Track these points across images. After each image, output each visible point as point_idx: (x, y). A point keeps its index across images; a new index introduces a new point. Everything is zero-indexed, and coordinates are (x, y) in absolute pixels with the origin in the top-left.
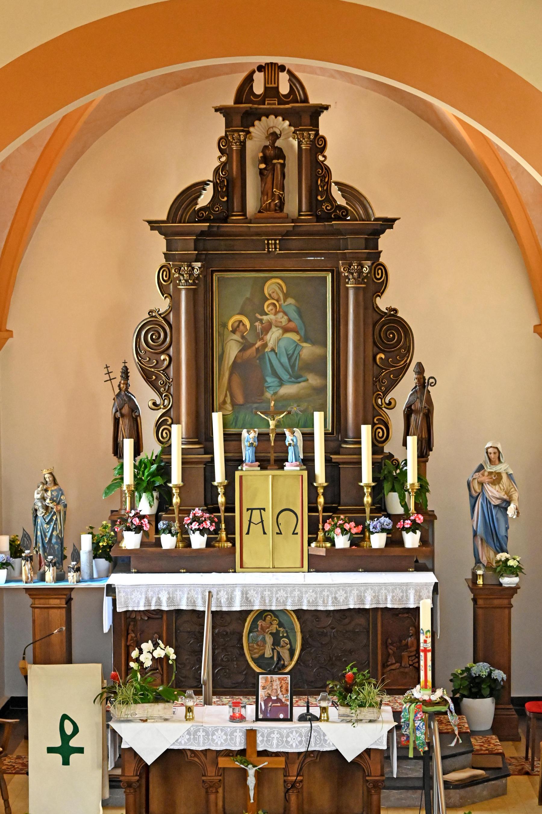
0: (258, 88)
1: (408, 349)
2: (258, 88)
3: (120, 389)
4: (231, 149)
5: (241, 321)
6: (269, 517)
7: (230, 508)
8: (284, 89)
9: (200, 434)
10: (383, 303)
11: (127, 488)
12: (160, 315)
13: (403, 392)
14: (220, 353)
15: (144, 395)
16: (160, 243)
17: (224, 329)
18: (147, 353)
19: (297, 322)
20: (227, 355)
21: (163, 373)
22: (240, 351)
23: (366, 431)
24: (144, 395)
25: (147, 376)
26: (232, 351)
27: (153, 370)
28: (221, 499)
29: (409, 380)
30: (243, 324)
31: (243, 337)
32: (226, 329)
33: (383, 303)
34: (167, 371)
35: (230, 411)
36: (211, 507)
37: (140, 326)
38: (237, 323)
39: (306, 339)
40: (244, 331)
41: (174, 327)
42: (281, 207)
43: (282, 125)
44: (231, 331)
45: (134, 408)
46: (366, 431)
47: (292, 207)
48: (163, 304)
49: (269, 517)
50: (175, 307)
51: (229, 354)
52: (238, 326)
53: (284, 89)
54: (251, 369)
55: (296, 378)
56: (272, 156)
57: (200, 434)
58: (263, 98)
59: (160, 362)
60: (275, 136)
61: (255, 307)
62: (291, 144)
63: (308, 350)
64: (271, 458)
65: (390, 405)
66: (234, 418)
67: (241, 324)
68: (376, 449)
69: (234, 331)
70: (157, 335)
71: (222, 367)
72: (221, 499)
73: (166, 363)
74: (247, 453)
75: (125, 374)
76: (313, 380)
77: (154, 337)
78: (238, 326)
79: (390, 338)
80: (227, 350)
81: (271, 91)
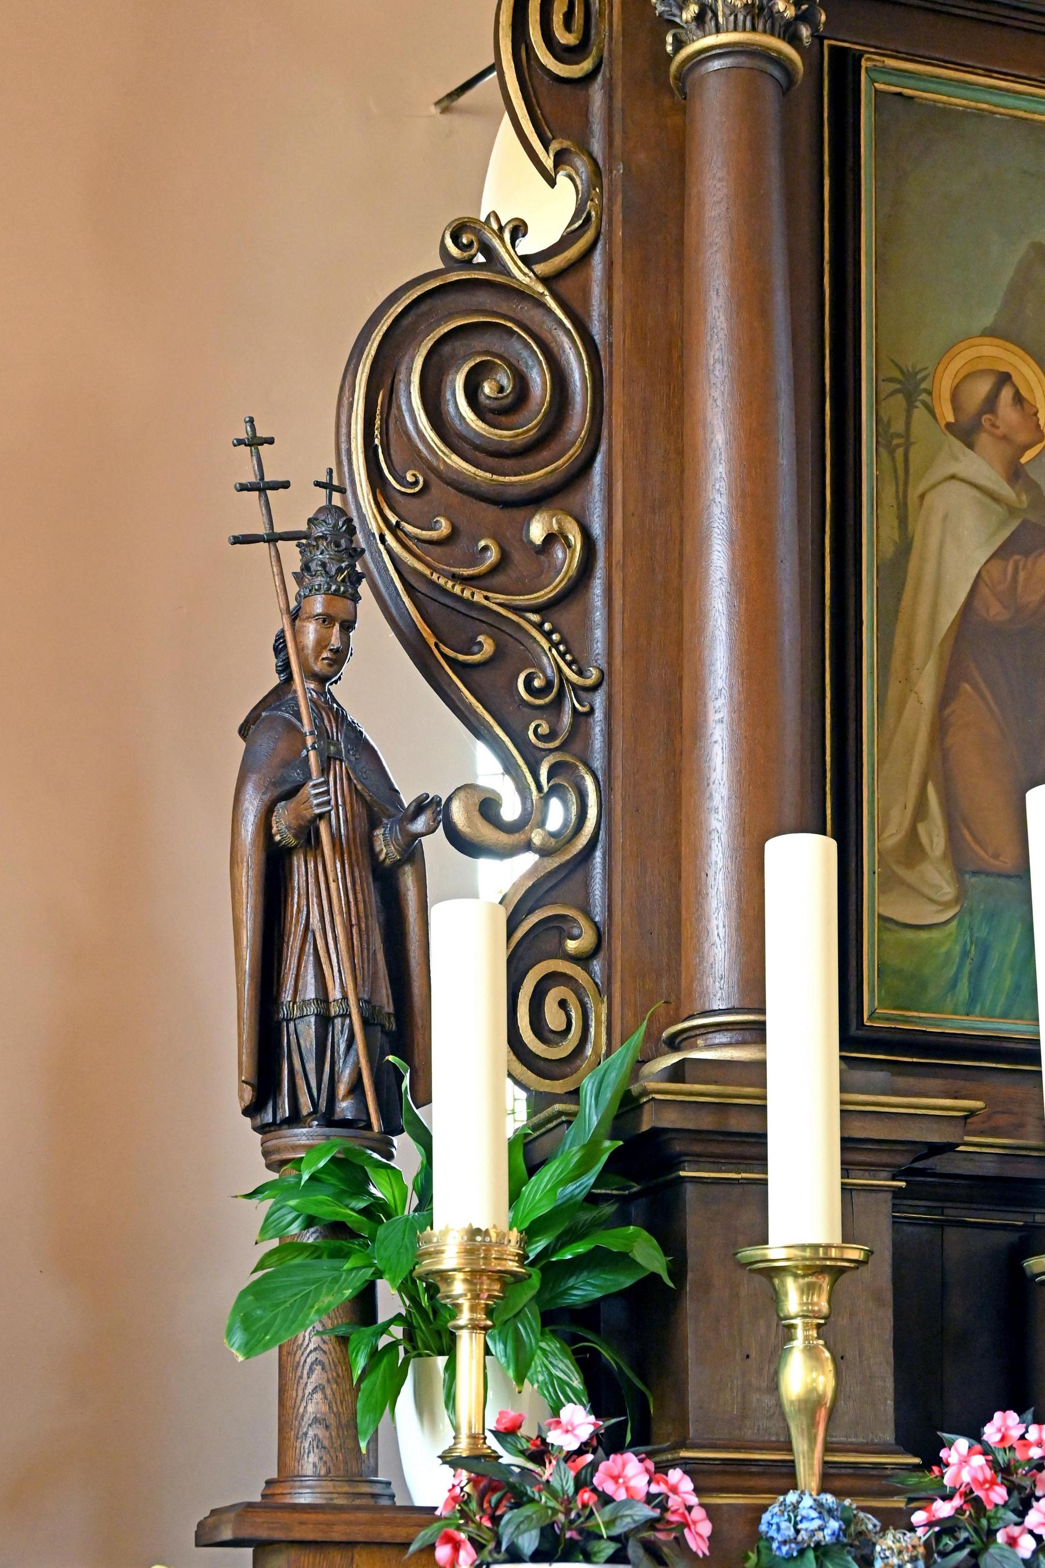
3: (285, 668)
5: (1004, 379)
11: (470, 1252)
14: (889, 551)
17: (910, 406)
18: (438, 489)
20: (930, 568)
21: (539, 627)
22: (1001, 553)
27: (478, 598)
30: (1018, 399)
31: (1015, 474)
32: (920, 414)
35: (947, 905)
38: (983, 388)
40: (1022, 438)
44: (948, 425)
51: (940, 563)
52: (991, 404)
59: (517, 556)
66: (965, 954)
67: (1006, 395)
69: (966, 433)
70: (505, 379)
71: (900, 629)
78: (991, 404)
80: (929, 537)
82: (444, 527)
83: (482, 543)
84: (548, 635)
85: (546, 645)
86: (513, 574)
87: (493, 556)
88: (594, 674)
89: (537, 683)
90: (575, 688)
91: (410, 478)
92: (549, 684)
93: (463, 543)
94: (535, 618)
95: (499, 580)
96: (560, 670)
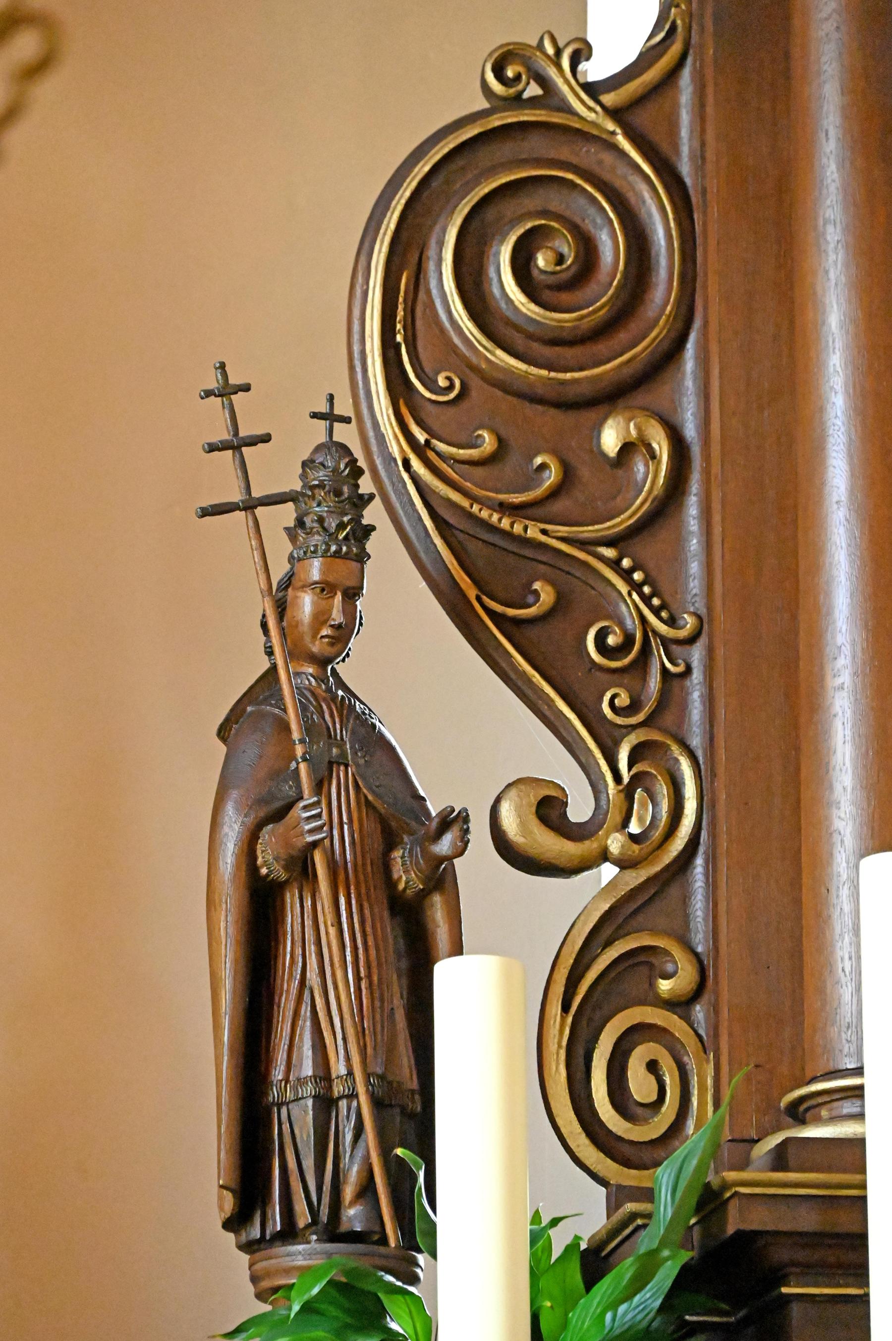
12: (592, 89)
21: (615, 564)
27: (533, 532)
34: (650, 548)
37: (424, 168)
73: (651, 476)
77: (542, 261)
82: (488, 442)
83: (538, 460)
84: (626, 575)
85: (623, 588)
86: (579, 494)
87: (552, 477)
88: (690, 621)
89: (611, 640)
90: (666, 642)
91: (442, 382)
92: (629, 640)
93: (514, 459)
94: (609, 553)
95: (559, 506)
96: (643, 620)
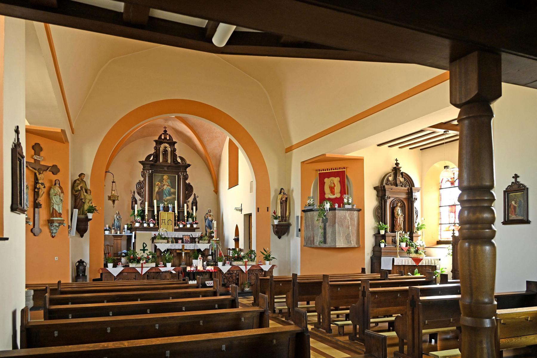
0: (163, 137)
1: (192, 191)
2: (163, 137)
4: (157, 149)
6: (166, 221)
7: (158, 220)
8: (168, 138)
9: (151, 205)
10: (187, 182)
13: (191, 199)
15: (138, 197)
16: (142, 167)
19: (170, 184)
23: (185, 205)
24: (138, 197)
25: (139, 194)
26: (156, 189)
28: (156, 218)
29: (192, 197)
33: (187, 182)
36: (154, 219)
39: (172, 188)
41: (145, 184)
42: (167, 161)
43: (167, 145)
45: (136, 200)
46: (185, 205)
47: (169, 161)
48: (142, 179)
49: (166, 221)
50: (145, 180)
53: (168, 138)
54: (161, 193)
55: (170, 195)
56: (165, 151)
57: (151, 205)
58: (164, 139)
60: (166, 147)
61: (161, 181)
62: (169, 149)
63: (172, 190)
64: (166, 209)
65: (189, 202)
68: (187, 209)
72: (156, 218)
74: (161, 209)
75: (134, 192)
76: (173, 196)
79: (189, 189)
81: (165, 138)
